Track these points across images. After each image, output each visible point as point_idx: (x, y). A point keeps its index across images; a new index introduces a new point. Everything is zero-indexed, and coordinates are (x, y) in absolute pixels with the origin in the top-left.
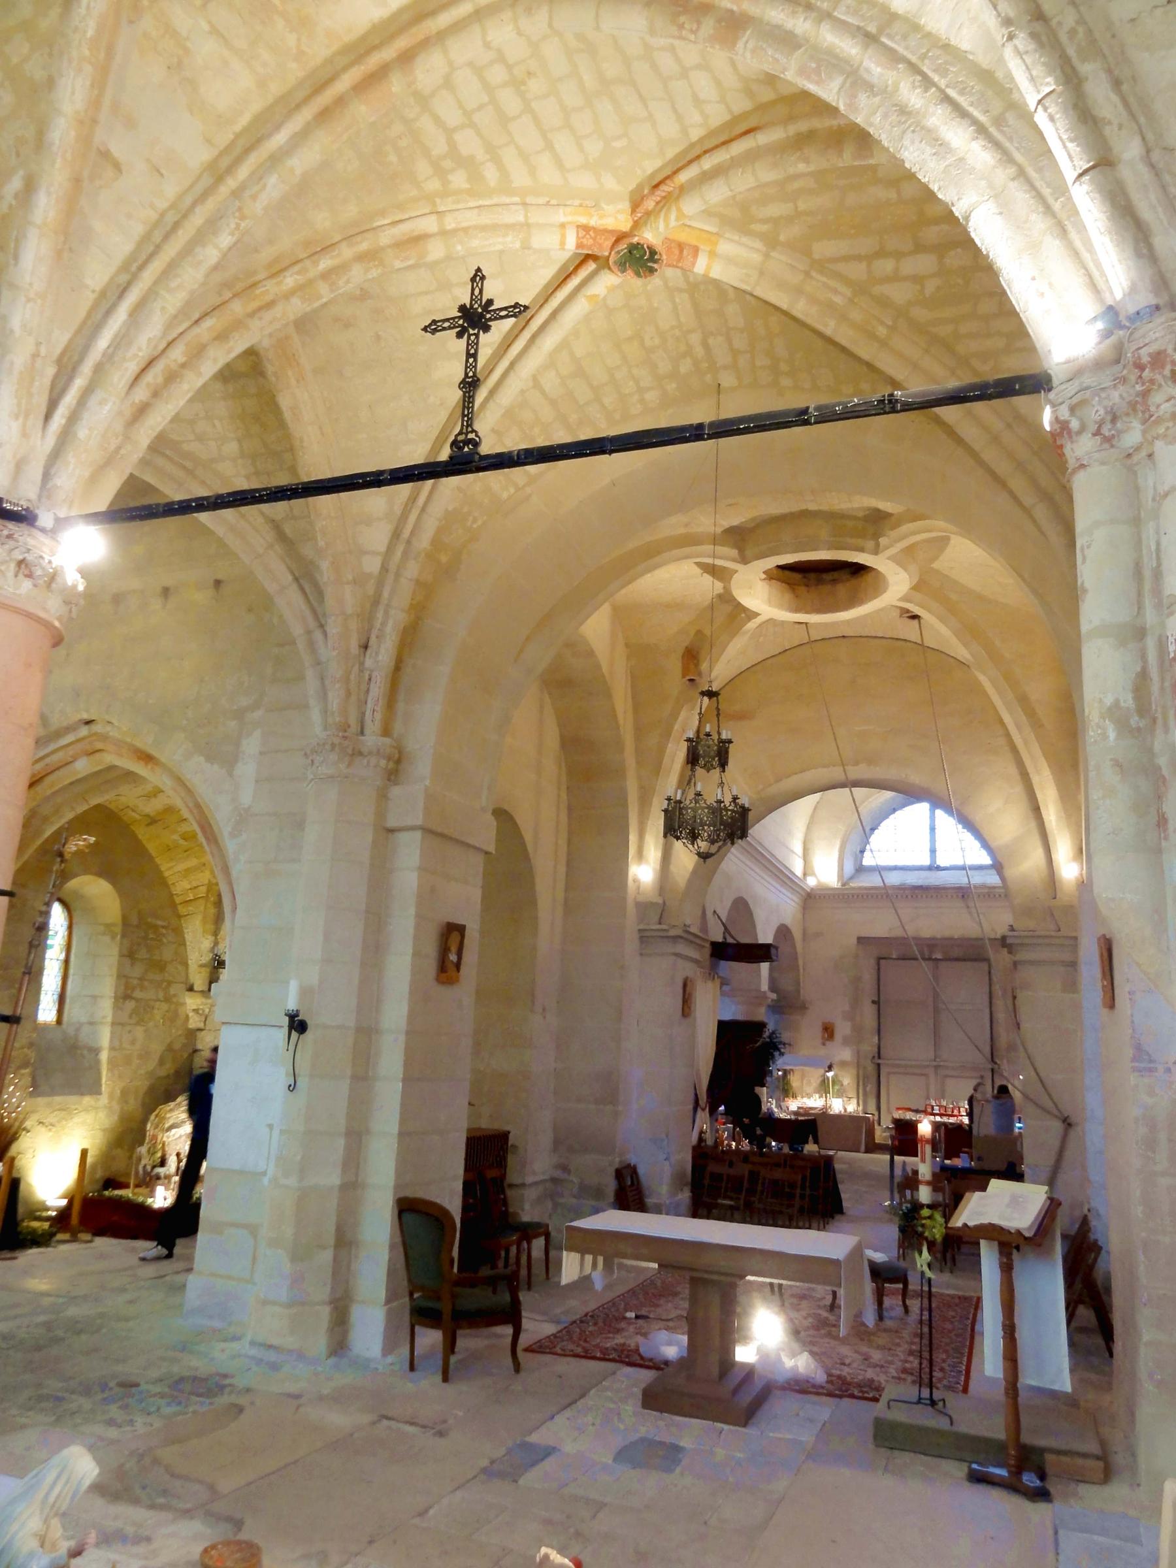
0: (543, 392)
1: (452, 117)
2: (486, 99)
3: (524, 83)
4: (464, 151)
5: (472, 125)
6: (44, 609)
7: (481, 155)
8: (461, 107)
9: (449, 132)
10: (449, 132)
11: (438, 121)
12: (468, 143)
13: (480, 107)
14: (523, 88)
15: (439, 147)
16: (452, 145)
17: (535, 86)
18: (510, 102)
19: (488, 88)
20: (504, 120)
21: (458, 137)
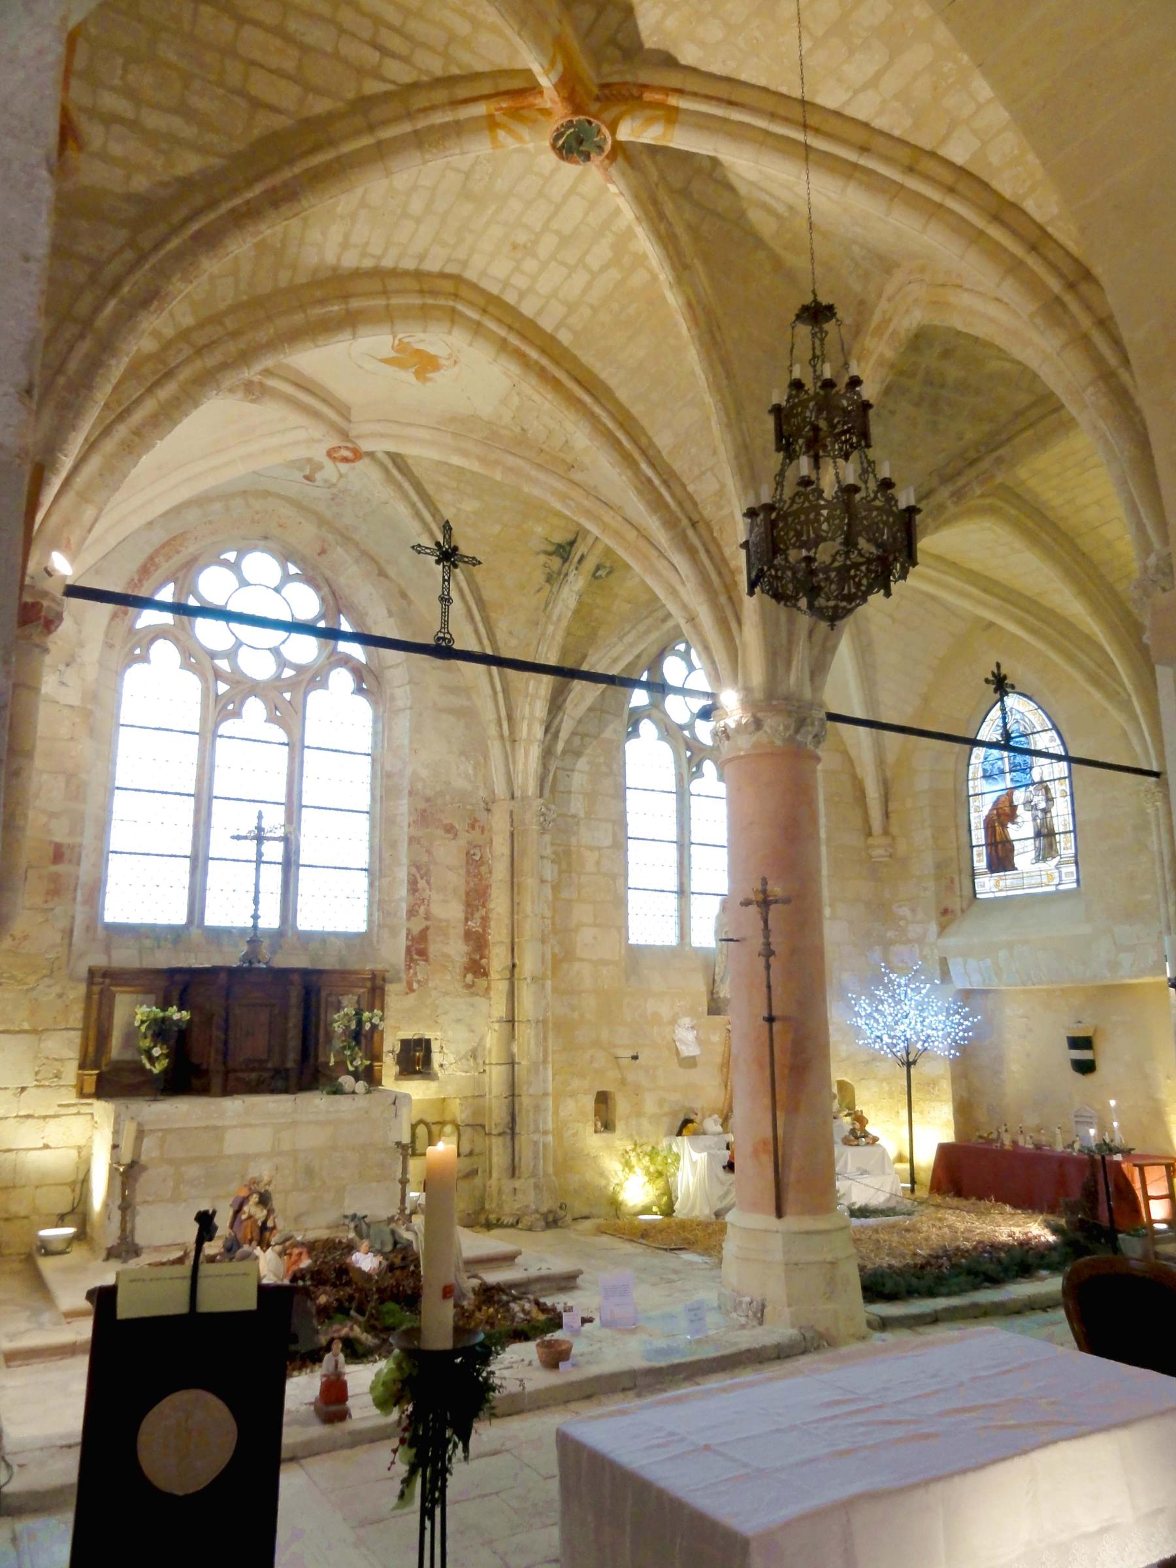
0: (878, 75)
1: (580, 280)
2: (553, 263)
3: (525, 247)
4: (609, 254)
5: (581, 260)
6: (740, 749)
7: (609, 239)
8: (569, 276)
9: (594, 275)
10: (594, 275)
11: (589, 285)
12: (602, 252)
13: (562, 263)
14: (529, 244)
15: (614, 274)
16: (604, 268)
17: (522, 237)
18: (548, 243)
19: (544, 266)
20: (565, 241)
21: (595, 266)
